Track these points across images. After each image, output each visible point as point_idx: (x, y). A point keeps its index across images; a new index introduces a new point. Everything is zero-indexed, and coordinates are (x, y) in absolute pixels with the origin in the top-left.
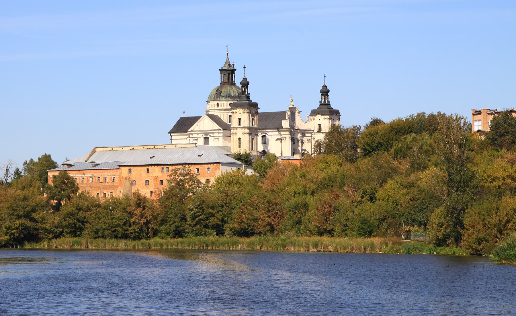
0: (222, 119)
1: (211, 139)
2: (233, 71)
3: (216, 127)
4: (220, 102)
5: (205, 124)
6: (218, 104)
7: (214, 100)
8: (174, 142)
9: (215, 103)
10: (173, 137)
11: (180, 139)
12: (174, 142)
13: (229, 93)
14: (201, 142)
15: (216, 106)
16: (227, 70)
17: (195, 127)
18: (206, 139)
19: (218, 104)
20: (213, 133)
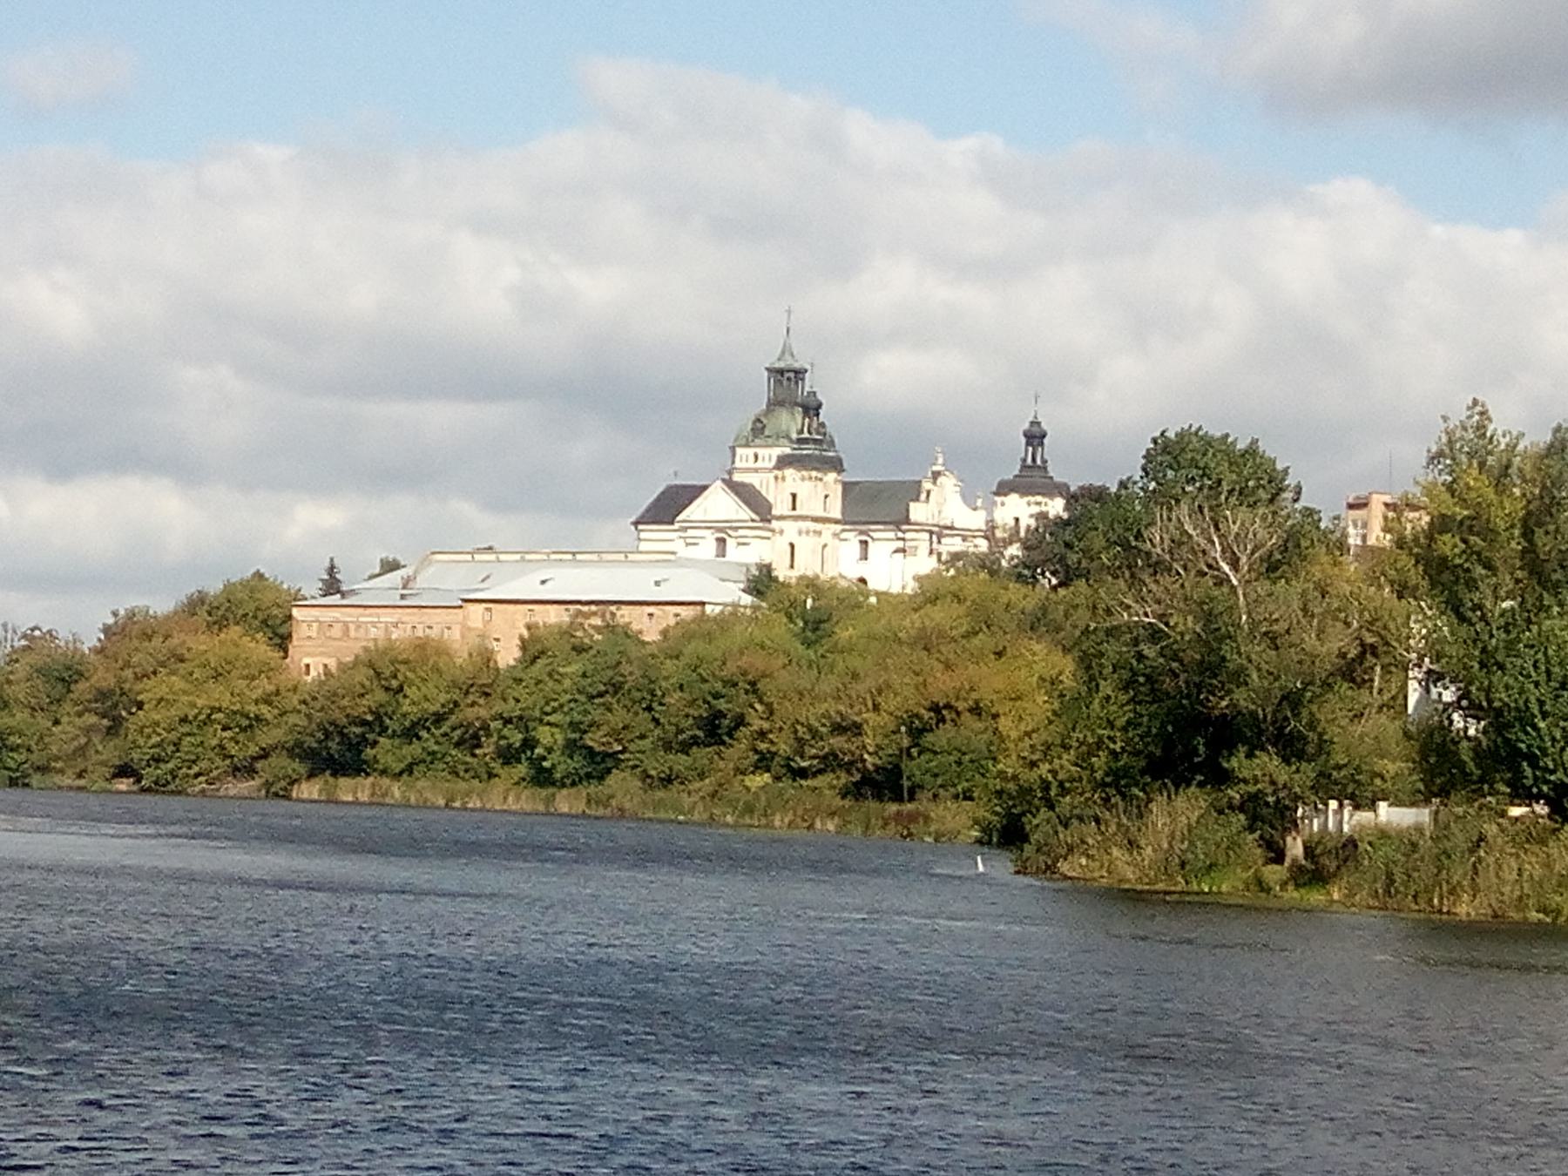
0: (764, 493)
1: (731, 543)
2: (799, 374)
3: (745, 513)
4: (761, 452)
5: (716, 504)
6: (756, 457)
7: (747, 445)
8: (643, 546)
9: (750, 452)
10: (643, 535)
11: (657, 538)
12: (643, 546)
13: (784, 427)
14: (708, 547)
15: (752, 458)
16: (781, 372)
17: (693, 512)
18: (721, 541)
19: (756, 457)
20: (737, 528)
